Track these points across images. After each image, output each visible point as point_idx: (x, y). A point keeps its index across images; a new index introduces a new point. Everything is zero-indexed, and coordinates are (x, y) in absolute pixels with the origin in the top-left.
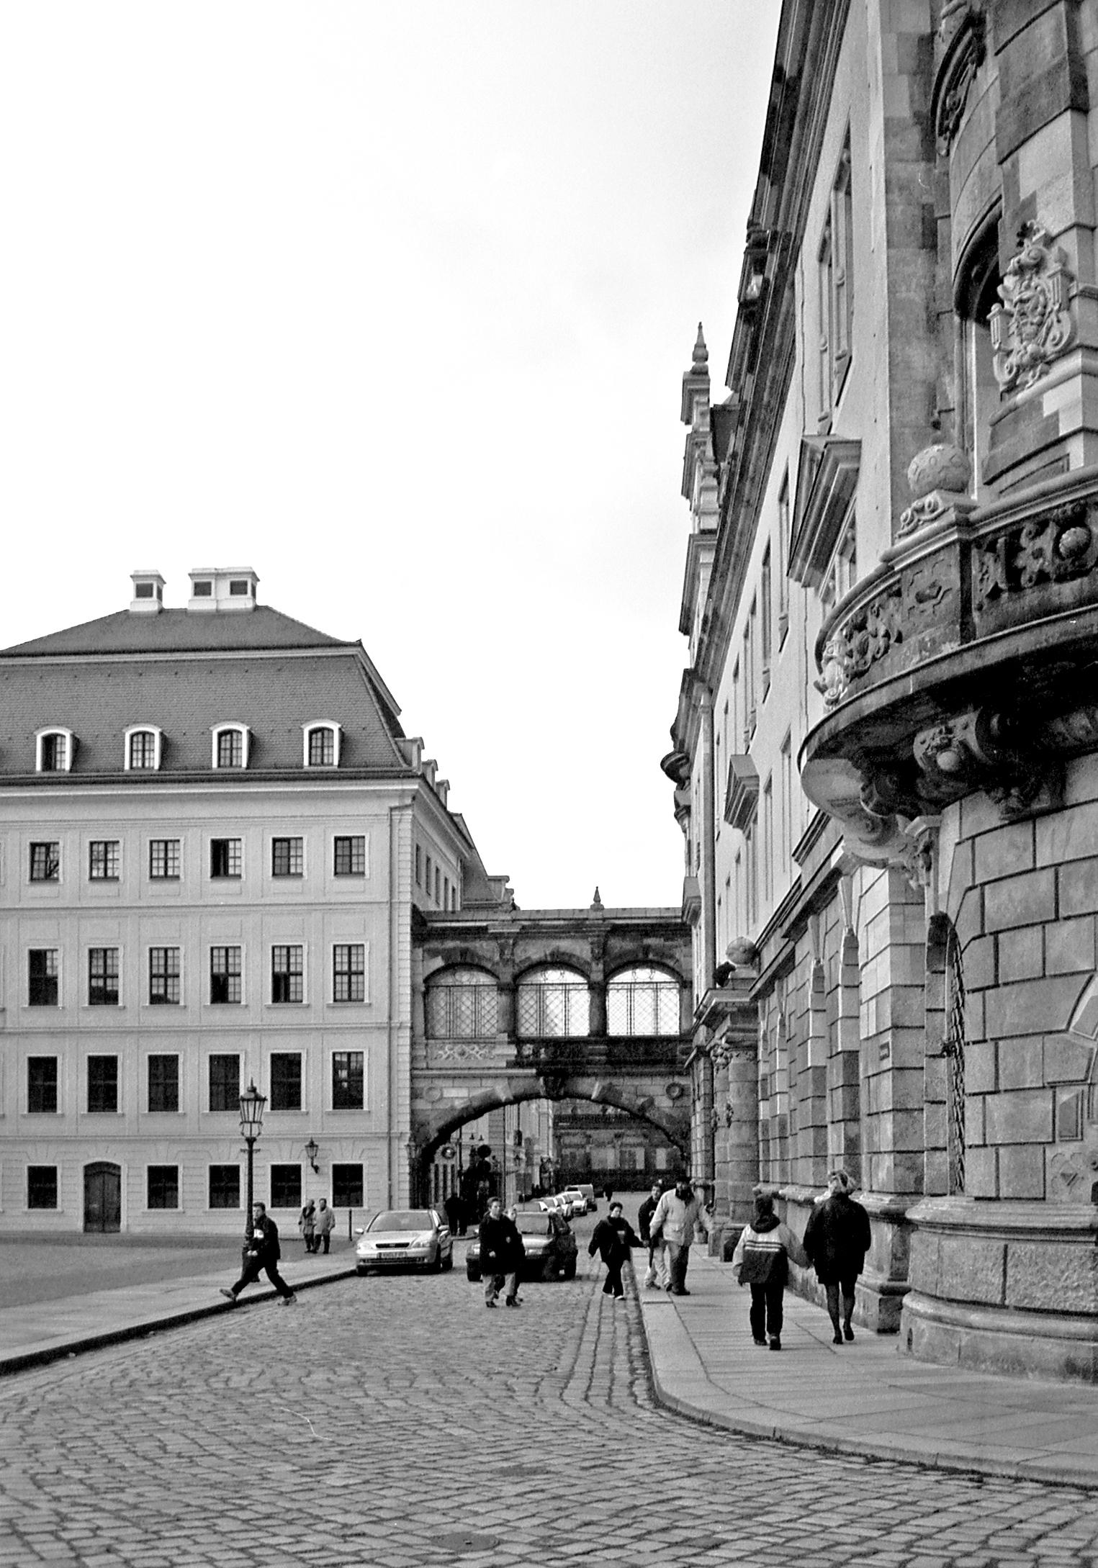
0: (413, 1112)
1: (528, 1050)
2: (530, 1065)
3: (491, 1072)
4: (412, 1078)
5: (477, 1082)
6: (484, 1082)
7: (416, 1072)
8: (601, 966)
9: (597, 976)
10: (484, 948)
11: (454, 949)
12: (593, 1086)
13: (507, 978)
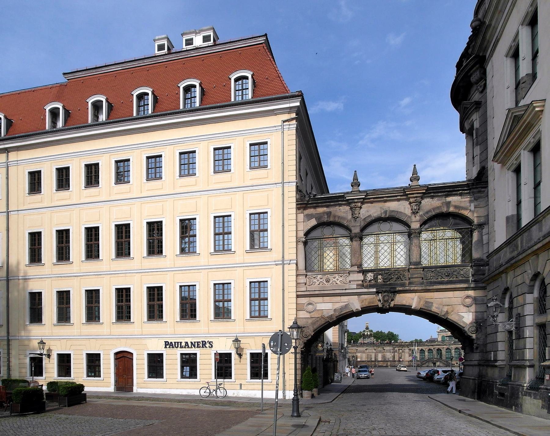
1: (370, 276)
8: (418, 218)
9: (415, 225)
10: (342, 212)
11: (324, 213)
13: (356, 230)
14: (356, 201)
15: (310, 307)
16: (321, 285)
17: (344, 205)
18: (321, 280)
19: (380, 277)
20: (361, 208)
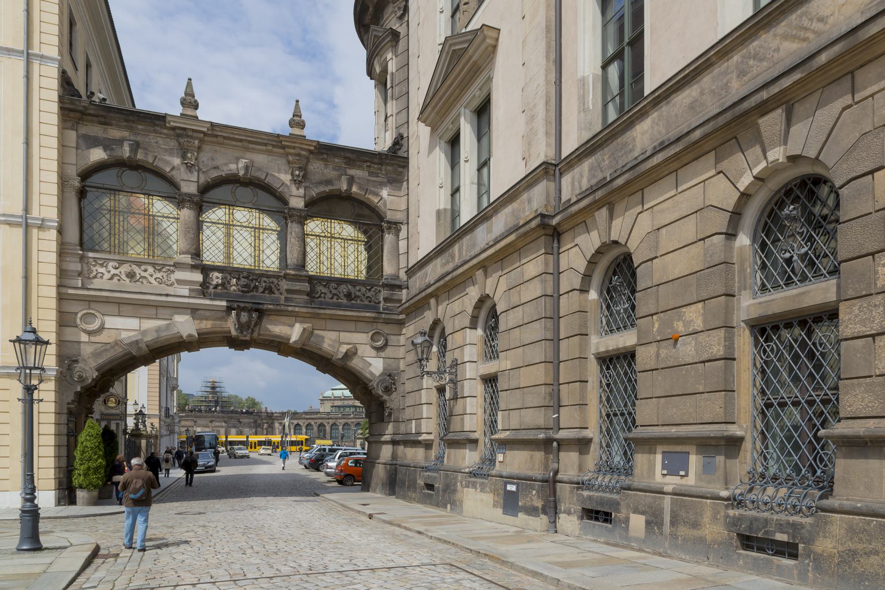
14: (190, 133)
17: (168, 136)
20: (199, 148)
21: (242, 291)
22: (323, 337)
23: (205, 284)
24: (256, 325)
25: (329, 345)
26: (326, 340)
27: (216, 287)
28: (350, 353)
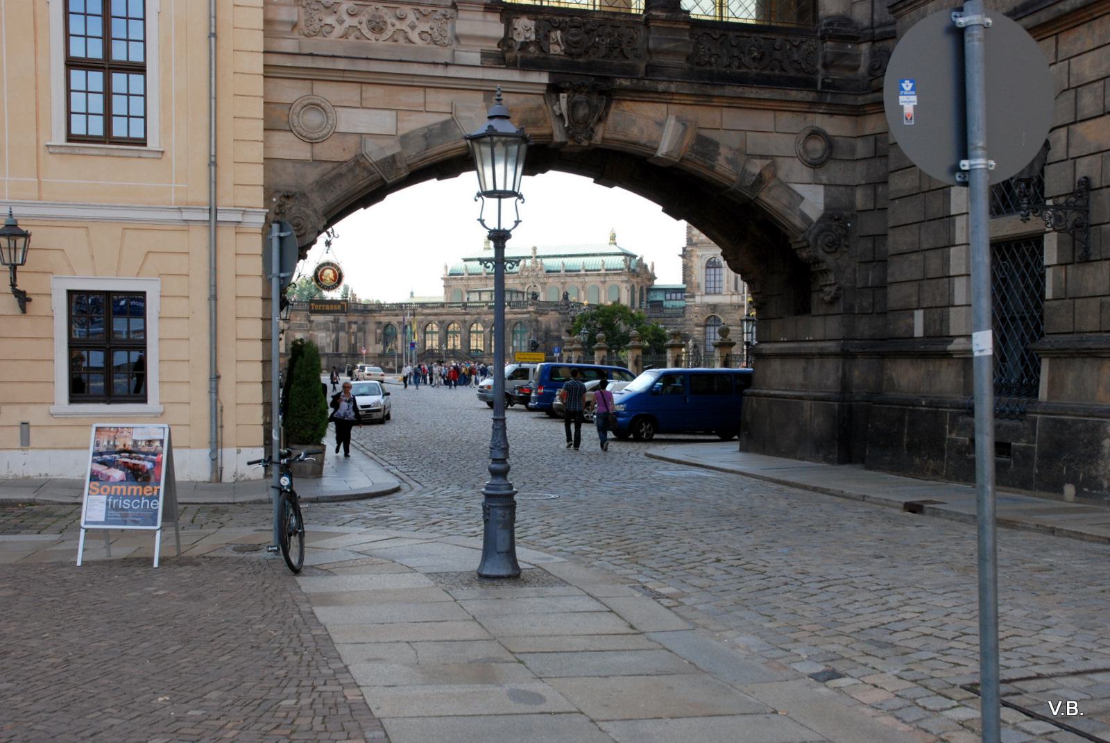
0: (268, 161)
2: (527, 65)
3: (452, 72)
4: (270, 73)
5: (416, 97)
6: (432, 95)
7: (275, 60)
12: (661, 125)
15: (313, 118)
16: (352, 38)
18: (354, 22)
19: (557, 35)
21: (571, 55)
22: (717, 145)
23: (506, 42)
24: (600, 120)
25: (729, 161)
26: (723, 150)
27: (525, 45)
28: (767, 175)
